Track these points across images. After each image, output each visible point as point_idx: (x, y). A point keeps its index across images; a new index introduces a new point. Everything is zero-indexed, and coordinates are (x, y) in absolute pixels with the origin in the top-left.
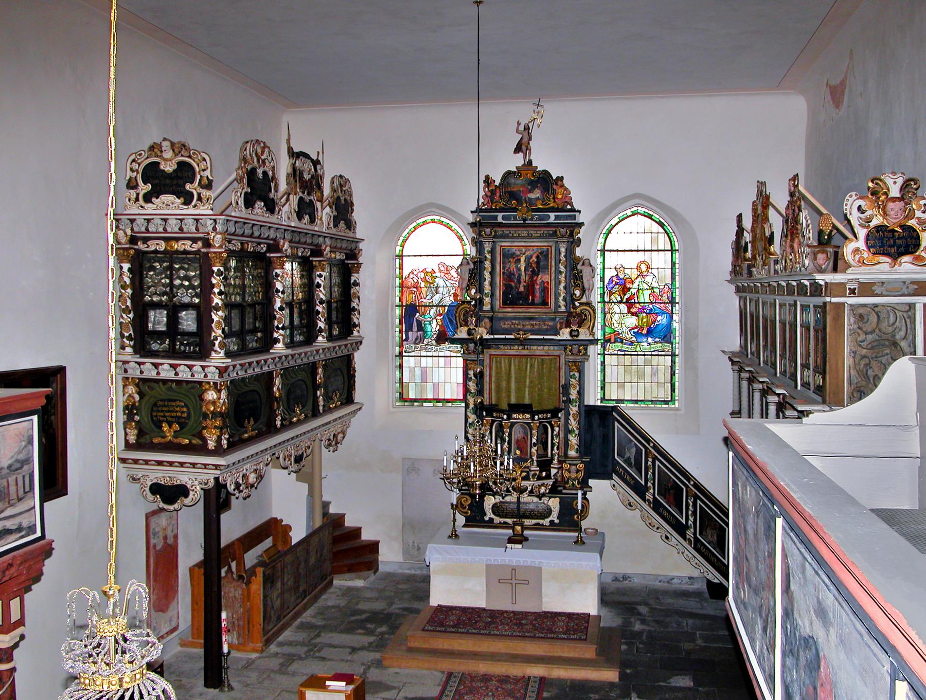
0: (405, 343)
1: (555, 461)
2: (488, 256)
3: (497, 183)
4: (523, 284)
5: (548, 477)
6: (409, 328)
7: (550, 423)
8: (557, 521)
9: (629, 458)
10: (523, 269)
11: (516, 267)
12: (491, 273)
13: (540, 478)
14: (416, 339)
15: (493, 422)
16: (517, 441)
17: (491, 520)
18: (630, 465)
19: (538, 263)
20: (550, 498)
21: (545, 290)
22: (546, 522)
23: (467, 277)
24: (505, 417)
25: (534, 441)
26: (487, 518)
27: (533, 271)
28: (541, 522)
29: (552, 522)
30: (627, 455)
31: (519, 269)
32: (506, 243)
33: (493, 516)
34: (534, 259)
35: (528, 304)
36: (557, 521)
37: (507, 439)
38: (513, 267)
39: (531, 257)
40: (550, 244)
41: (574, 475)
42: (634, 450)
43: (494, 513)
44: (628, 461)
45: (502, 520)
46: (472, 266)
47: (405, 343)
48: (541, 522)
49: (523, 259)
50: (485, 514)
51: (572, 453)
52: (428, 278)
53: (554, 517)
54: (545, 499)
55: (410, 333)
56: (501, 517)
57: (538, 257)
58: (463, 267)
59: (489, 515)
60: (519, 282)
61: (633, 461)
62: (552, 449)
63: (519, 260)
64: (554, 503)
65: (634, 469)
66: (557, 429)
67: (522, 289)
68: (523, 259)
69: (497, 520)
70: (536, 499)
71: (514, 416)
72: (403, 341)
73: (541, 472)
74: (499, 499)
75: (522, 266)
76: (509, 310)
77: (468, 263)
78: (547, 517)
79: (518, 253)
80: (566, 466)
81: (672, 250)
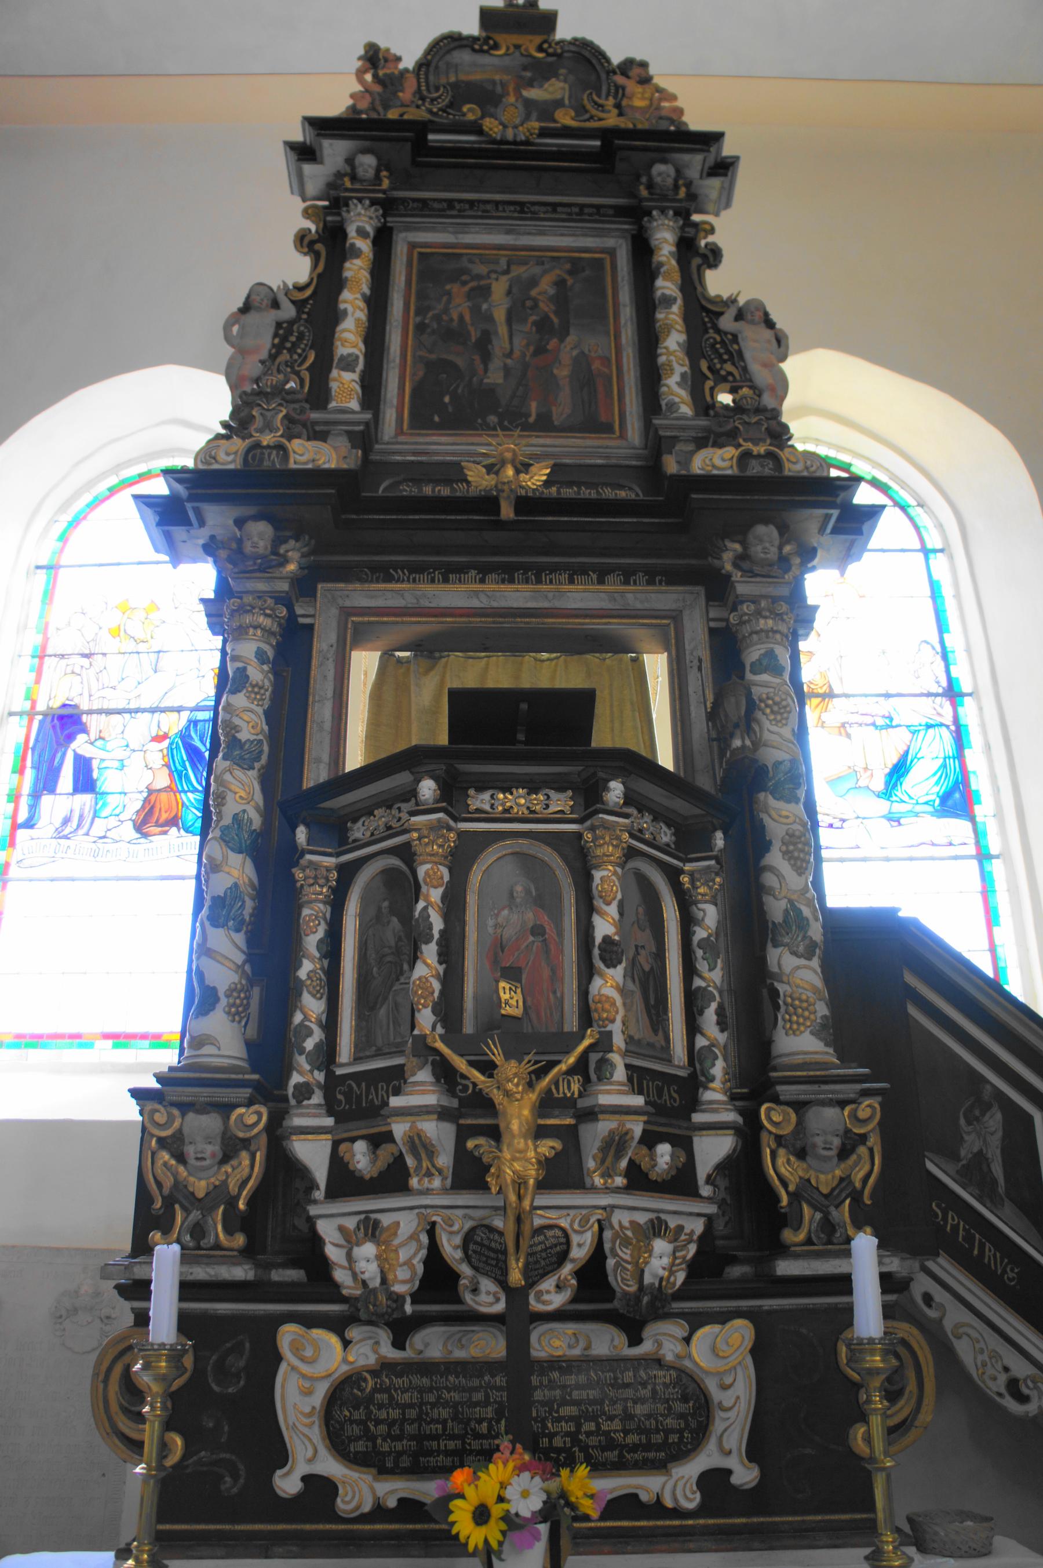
0: (21, 833)
1: (714, 1094)
2: (365, 246)
3: (408, 62)
4: (496, 364)
5: (681, 1183)
6: (47, 783)
7: (673, 875)
8: (745, 1475)
9: (980, 1157)
10: (500, 315)
11: (475, 310)
12: (368, 300)
13: (639, 1180)
14: (66, 821)
15: (347, 873)
16: (499, 946)
17: (320, 1489)
18: (987, 1191)
19: (562, 296)
20: (696, 1321)
21: (589, 381)
22: (678, 1485)
23: (265, 342)
24: (428, 788)
25: (604, 927)
26: (288, 1484)
27: (543, 326)
28: (648, 1485)
29: (714, 1481)
30: (971, 1144)
31: (489, 318)
32: (435, 236)
33: (330, 1466)
34: (546, 286)
35: (526, 427)
36: (745, 1475)
37: (437, 924)
38: (460, 307)
39: (533, 282)
40: (610, 242)
41: (825, 1181)
42: (994, 1120)
43: (338, 1442)
44: (975, 1172)
45: (391, 1490)
46: (288, 311)
47: (21, 833)
48: (648, 1485)
49: (499, 288)
50: (280, 1456)
51: (800, 1043)
52: (135, 628)
53: (727, 1447)
54: (664, 1338)
55: (46, 800)
56: (383, 1472)
57: (560, 283)
58: (251, 318)
59: (308, 1455)
60: (486, 357)
61: (997, 1170)
62: (693, 1028)
63: (484, 292)
64: (720, 1354)
65: (1009, 1209)
66: (710, 915)
67: (495, 377)
68: (499, 288)
69: (359, 1490)
70: (605, 1341)
71: (481, 800)
72: (15, 827)
73: (649, 1140)
74: (371, 1348)
75: (499, 305)
76: (443, 439)
77: (275, 304)
78: (681, 1453)
79: (481, 269)
80: (774, 1118)
81: (925, 551)
